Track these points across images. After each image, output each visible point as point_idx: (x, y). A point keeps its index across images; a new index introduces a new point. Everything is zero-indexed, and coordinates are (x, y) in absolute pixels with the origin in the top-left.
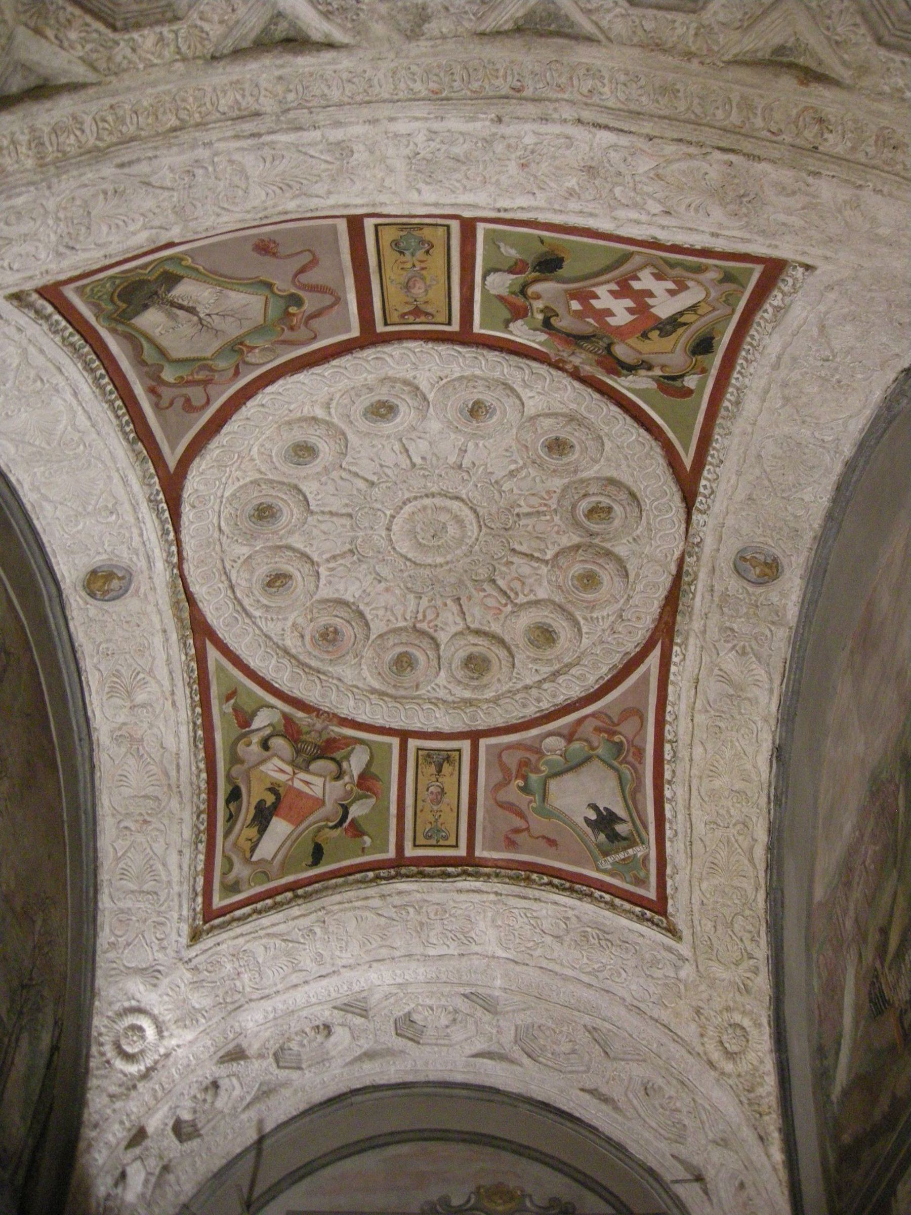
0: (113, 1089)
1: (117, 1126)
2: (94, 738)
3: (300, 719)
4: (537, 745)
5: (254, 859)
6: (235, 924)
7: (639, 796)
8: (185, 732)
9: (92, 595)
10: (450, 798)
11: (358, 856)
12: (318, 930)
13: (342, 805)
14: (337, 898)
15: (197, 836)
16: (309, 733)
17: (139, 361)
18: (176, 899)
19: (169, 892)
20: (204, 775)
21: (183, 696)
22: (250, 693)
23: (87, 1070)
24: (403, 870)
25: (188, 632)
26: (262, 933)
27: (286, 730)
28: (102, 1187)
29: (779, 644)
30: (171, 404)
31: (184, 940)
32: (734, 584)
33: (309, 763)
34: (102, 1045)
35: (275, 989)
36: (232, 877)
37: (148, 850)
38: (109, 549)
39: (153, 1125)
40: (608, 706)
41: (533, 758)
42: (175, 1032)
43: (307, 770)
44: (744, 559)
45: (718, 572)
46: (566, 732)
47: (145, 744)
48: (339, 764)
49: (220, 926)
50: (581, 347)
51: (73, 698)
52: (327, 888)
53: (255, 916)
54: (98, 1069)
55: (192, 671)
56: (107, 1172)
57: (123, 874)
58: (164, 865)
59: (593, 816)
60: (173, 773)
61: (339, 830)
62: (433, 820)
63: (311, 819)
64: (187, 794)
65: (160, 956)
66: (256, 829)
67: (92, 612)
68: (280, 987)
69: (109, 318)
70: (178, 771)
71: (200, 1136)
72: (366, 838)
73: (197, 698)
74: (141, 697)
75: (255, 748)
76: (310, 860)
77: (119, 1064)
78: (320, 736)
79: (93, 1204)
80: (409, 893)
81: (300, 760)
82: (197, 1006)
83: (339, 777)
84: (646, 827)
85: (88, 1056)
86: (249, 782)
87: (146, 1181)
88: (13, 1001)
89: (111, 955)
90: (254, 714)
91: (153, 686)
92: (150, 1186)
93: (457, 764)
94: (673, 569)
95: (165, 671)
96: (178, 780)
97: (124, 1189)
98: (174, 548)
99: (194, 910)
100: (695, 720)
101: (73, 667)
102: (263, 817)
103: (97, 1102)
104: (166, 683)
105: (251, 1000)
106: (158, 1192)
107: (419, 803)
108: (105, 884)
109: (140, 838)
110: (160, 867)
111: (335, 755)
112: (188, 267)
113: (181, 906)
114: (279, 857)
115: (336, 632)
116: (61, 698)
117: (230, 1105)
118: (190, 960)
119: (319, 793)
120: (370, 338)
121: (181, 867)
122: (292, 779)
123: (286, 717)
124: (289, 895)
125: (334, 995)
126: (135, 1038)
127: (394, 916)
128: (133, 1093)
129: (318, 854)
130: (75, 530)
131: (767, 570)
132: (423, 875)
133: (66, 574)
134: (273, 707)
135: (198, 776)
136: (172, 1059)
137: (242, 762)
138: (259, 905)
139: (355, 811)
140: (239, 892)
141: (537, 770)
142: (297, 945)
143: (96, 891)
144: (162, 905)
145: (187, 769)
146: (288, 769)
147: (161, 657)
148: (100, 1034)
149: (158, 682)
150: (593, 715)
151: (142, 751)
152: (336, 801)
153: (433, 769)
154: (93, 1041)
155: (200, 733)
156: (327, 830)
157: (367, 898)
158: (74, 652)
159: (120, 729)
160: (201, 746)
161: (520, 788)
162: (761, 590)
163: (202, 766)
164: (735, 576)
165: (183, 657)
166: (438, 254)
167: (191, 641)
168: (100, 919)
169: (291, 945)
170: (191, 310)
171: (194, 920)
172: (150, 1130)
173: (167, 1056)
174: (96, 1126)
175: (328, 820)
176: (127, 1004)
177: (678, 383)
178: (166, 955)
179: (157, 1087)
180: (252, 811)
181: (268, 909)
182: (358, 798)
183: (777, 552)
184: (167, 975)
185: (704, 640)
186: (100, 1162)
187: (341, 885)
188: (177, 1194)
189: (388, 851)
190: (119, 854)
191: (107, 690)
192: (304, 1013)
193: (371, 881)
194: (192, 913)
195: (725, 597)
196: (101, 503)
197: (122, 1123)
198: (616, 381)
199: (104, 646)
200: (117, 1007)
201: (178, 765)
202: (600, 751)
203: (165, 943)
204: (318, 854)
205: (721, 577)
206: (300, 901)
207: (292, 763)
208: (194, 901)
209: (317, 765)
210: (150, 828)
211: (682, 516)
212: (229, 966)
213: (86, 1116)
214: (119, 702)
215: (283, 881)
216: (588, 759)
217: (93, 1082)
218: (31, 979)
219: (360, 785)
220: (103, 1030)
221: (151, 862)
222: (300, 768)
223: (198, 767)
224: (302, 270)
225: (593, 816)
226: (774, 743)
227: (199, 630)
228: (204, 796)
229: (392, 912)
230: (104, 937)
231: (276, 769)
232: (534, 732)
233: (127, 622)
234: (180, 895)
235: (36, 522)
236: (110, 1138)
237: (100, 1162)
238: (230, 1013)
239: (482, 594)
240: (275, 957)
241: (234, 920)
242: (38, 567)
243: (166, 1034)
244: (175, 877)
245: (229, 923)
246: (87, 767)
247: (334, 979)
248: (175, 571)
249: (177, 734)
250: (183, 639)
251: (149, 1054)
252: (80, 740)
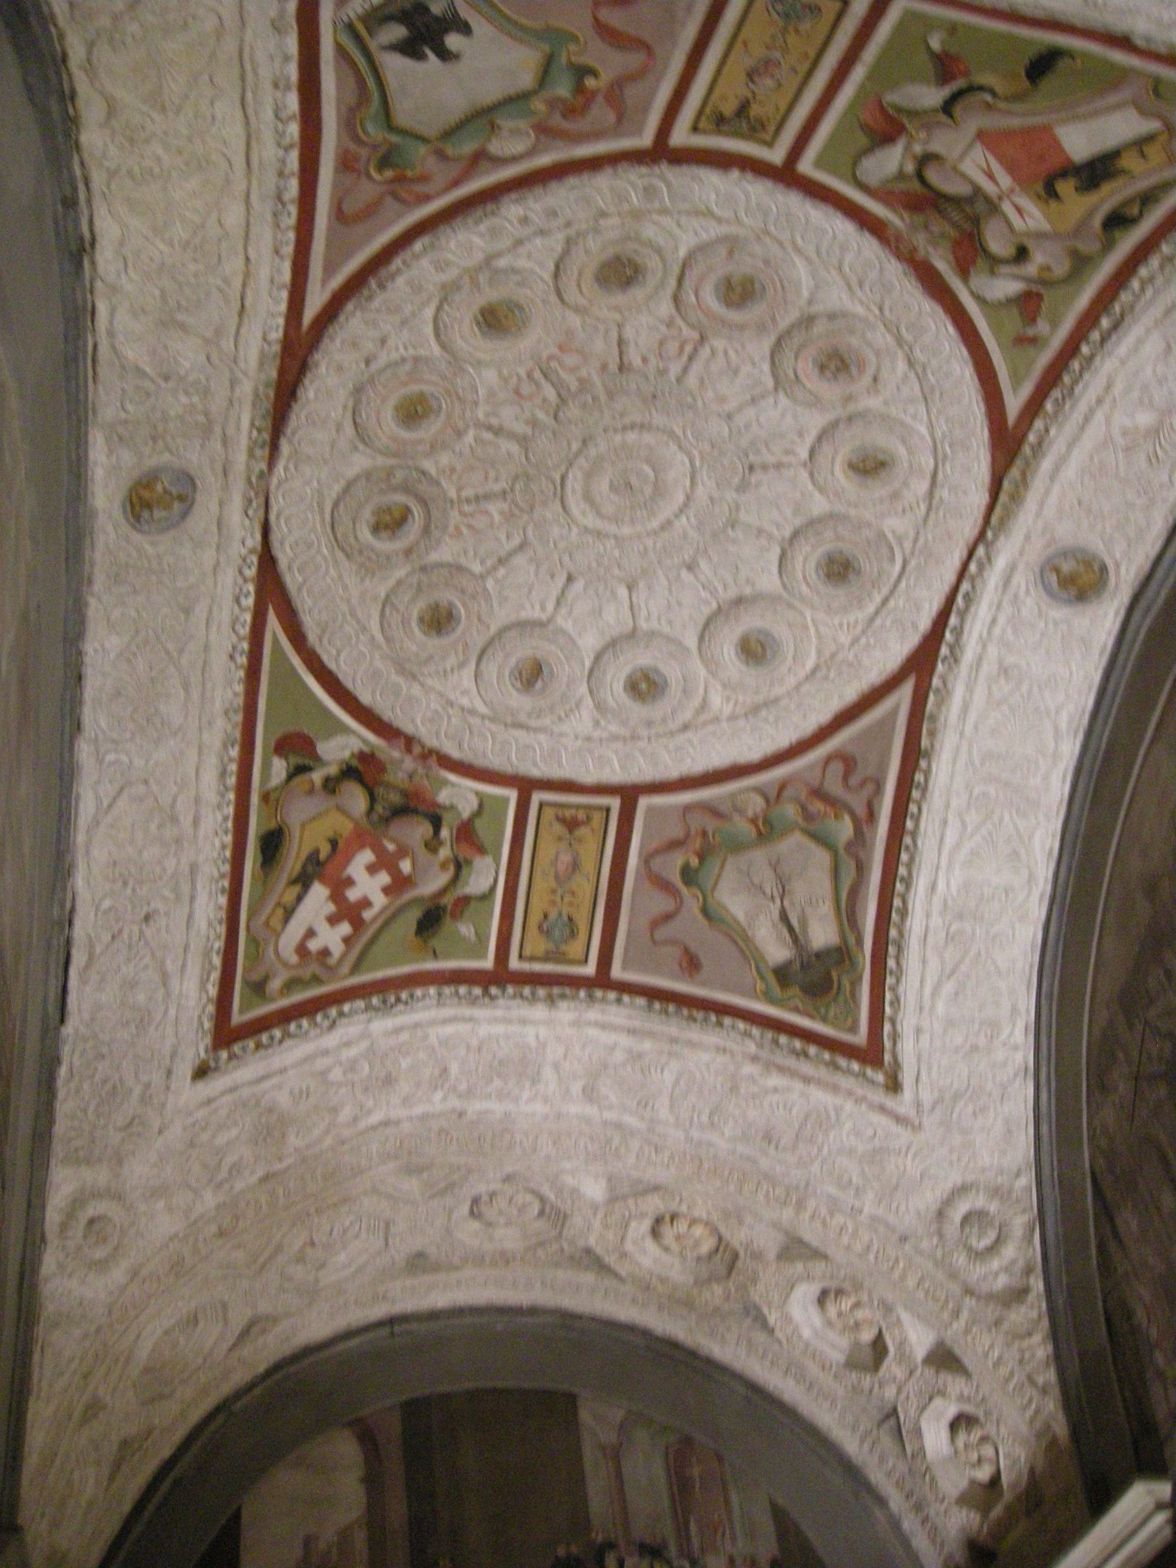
4: (542, 138)
7: (352, 99)
8: (1124, 345)
9: (1104, 569)
10: (741, 61)
16: (943, 235)
17: (861, 869)
20: (1143, 272)
21: (1090, 388)
25: (1027, 449)
29: (109, 400)
30: (862, 784)
32: (194, 457)
33: (970, 200)
40: (400, 216)
41: (557, 120)
43: (977, 190)
44: (181, 498)
45: (219, 468)
46: (484, 164)
50: (405, 794)
59: (453, 41)
63: (1015, 122)
69: (853, 964)
72: (935, 44)
75: (1039, 257)
76: (1063, 64)
81: (980, 207)
84: (340, 49)
90: (1010, 301)
91: (1120, 420)
93: (708, 110)
94: (285, 448)
98: (973, 567)
100: (242, 258)
102: (1097, 171)
104: (1099, 416)
112: (762, 978)
114: (1113, 99)
115: (822, 368)
119: (978, 152)
120: (630, 794)
123: (964, 272)
131: (146, 494)
133: (1111, 614)
139: (931, 96)
141: (552, 104)
146: (1007, 207)
150: (427, 198)
153: (755, 110)
155: (1105, 323)
156: (998, 89)
161: (594, 73)
162: (151, 462)
163: (1135, 284)
164: (192, 472)
165: (1053, 432)
166: (535, 918)
170: (784, 917)
175: (989, 106)
177: (295, 760)
180: (1106, 188)
182: (914, 114)
183: (136, 537)
185: (232, 371)
195: (206, 431)
198: (364, 741)
202: (422, 150)
205: (212, 461)
207: (993, 208)
211: (275, 537)
215: (1134, 61)
216: (449, 134)
219: (900, 129)
223: (1143, 289)
224: (668, 917)
225: (453, 41)
226: (93, 263)
227: (1009, 444)
232: (544, 160)
239: (584, 373)
242: (1106, 722)
248: (989, 534)
249: (1136, 349)
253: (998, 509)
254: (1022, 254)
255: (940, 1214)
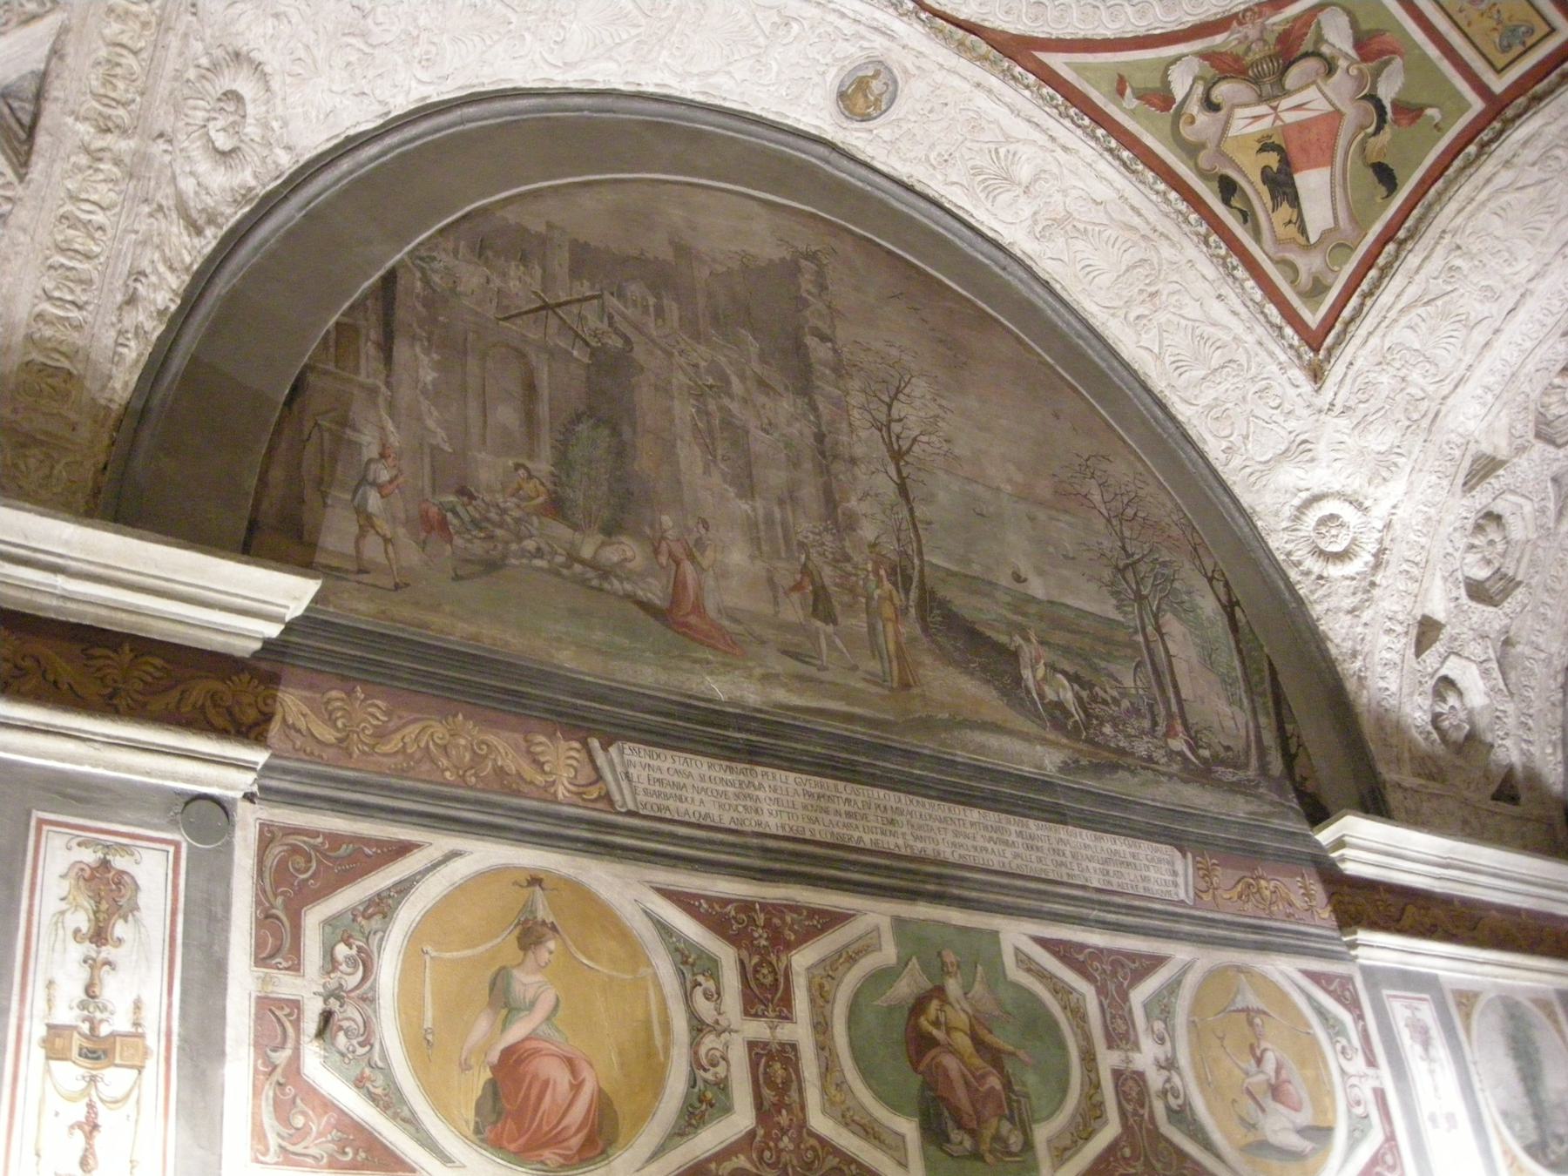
0: (1348, 603)
1: (1385, 639)
2: (1019, 254)
3: (1225, 42)
5: (1313, 239)
6: (1352, 328)
8: (1106, 167)
9: (866, 118)
11: (1439, 139)
12: (1458, 262)
13: (1364, 97)
14: (1452, 206)
15: (1225, 265)
16: (1249, 49)
18: (1258, 348)
19: (1246, 350)
20: (1173, 195)
21: (1067, 133)
22: (1136, 65)
23: (1300, 601)
24: (1509, 112)
25: (1006, 63)
26: (1393, 314)
27: (1222, 71)
28: (1417, 712)
31: (1307, 387)
34: (1299, 563)
35: (1463, 366)
36: (1304, 278)
37: (1183, 322)
38: (829, 59)
39: (1438, 608)
42: (1379, 493)
43: (1287, 93)
47: (1075, 215)
48: (1316, 54)
49: (1338, 342)
51: (955, 234)
52: (1430, 206)
53: (1369, 302)
54: (1312, 592)
55: (1052, 98)
56: (1411, 694)
57: (1178, 366)
58: (1214, 325)
60: (1136, 221)
61: (1387, 128)
62: (1492, 24)
63: (1342, 142)
64: (1168, 227)
65: (1292, 424)
66: (1285, 205)
67: (886, 134)
68: (1468, 359)
70: (1140, 215)
71: (1519, 584)
73: (1087, 121)
74: (1024, 173)
75: (1203, 118)
76: (1383, 190)
77: (1334, 571)
78: (1265, 42)
79: (1420, 738)
80: (1536, 135)
81: (1267, 89)
82: (1383, 448)
83: (1330, 69)
85: (1291, 587)
86: (1232, 161)
87: (1485, 673)
88: (1116, 594)
89: (1236, 462)
90: (1166, 84)
91: (1025, 151)
92: (1496, 674)
95: (1024, 126)
96: (1148, 223)
97: (1460, 694)
99: (1291, 346)
101: (923, 204)
102: (1282, 186)
103: (1338, 630)
104: (1036, 135)
105: (1444, 398)
106: (1513, 676)
107: (1459, 18)
108: (1167, 392)
109: (1162, 317)
110: (1212, 329)
111: (1303, 49)
113: (1271, 354)
114: (1342, 215)
116: (936, 244)
117: (1531, 527)
118: (1332, 405)
121: (1235, 313)
122: (1277, 117)
123: (1204, 56)
124: (1391, 247)
125: (1550, 321)
126: (1334, 532)
127: (1543, 176)
128: (1376, 592)
129: (1386, 177)
130: (773, 75)
132: (1538, 99)
134: (1179, 58)
135: (1167, 201)
136: (1397, 526)
137: (1202, 146)
138: (1364, 286)
139: (1388, 91)
140: (1327, 288)
142: (1446, 298)
143: (1163, 407)
144: (1249, 369)
145: (1150, 206)
146: (1263, 109)
147: (1001, 113)
148: (1289, 554)
149: (1025, 142)
151: (1081, 226)
152: (1353, 99)
154: (1284, 565)
155: (1126, 154)
157: (1488, 181)
158: (909, 189)
159: (1035, 222)
160: (1140, 167)
163: (1161, 186)
165: (1027, 93)
167: (1018, 69)
168: (1192, 433)
169: (1439, 302)
171: (1300, 357)
172: (1440, 616)
173: (1388, 526)
174: (1354, 654)
175: (1363, 128)
176: (1296, 502)
178: (1299, 418)
179: (1405, 566)
180: (1264, 190)
181: (1377, 284)
182: (1377, 74)
184: (1318, 438)
186: (1394, 688)
187: (1446, 189)
188: (1548, 662)
189: (1469, 106)
190: (1156, 350)
191: (983, 196)
192: (1530, 367)
193: (1478, 156)
194: (1291, 353)
196: (767, 28)
197: (1389, 631)
199: (933, 156)
200: (1287, 511)
201: (1133, 208)
203: (1287, 407)
204: (1386, 177)
206: (1409, 246)
207: (1261, 99)
208: (1283, 337)
209: (1293, 77)
210: (1164, 297)
212: (1384, 379)
213: (1334, 651)
214: (1005, 198)
217: (1316, 610)
218: (1129, 556)
219: (1365, 58)
220: (1289, 547)
221: (1198, 332)
222: (1276, 97)
223: (1157, 193)
227: (1016, 51)
228: (1193, 217)
229: (1535, 173)
230: (1214, 450)
231: (1249, 121)
233: (931, 111)
234: (1260, 344)
235: (727, 104)
236: (1388, 655)
237: (1394, 688)
238: (1430, 431)
240: (1432, 331)
241: (1347, 324)
243: (1367, 504)
244: (1238, 327)
245: (1345, 331)
246: (1038, 289)
247: (1530, 303)
248: (923, 15)
249: (1100, 177)
250: (1007, 75)
251: (1364, 538)
252: (1004, 269)
253: (948, 27)
254: (1210, 106)
255: (1317, 498)
